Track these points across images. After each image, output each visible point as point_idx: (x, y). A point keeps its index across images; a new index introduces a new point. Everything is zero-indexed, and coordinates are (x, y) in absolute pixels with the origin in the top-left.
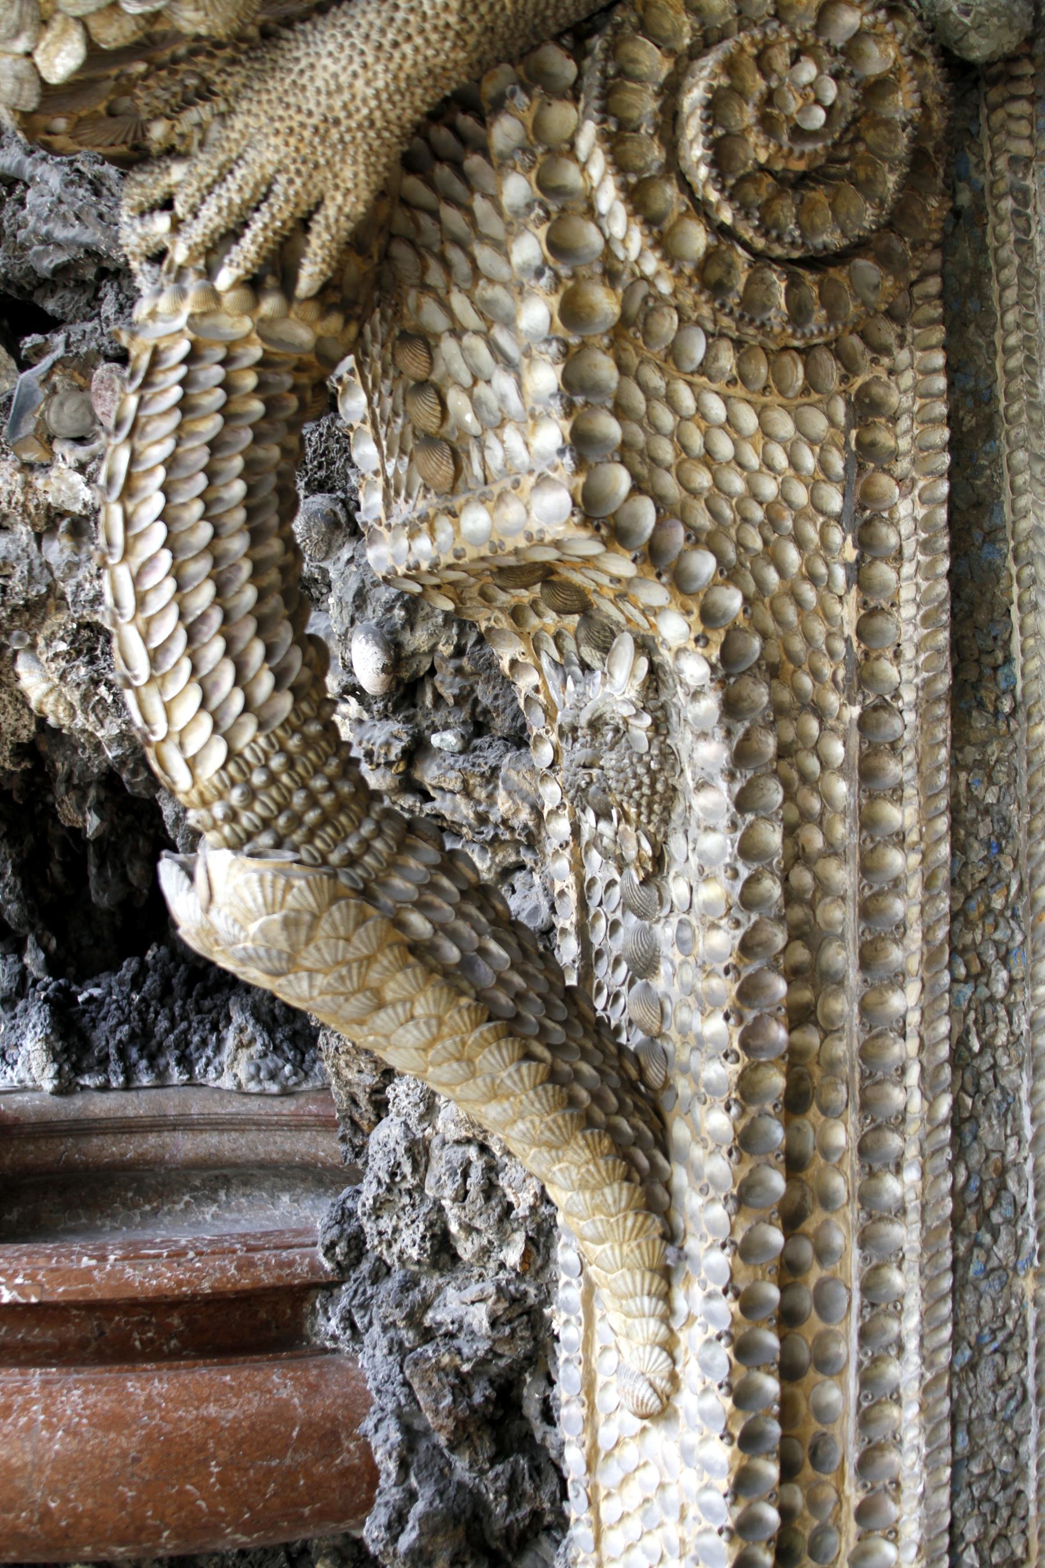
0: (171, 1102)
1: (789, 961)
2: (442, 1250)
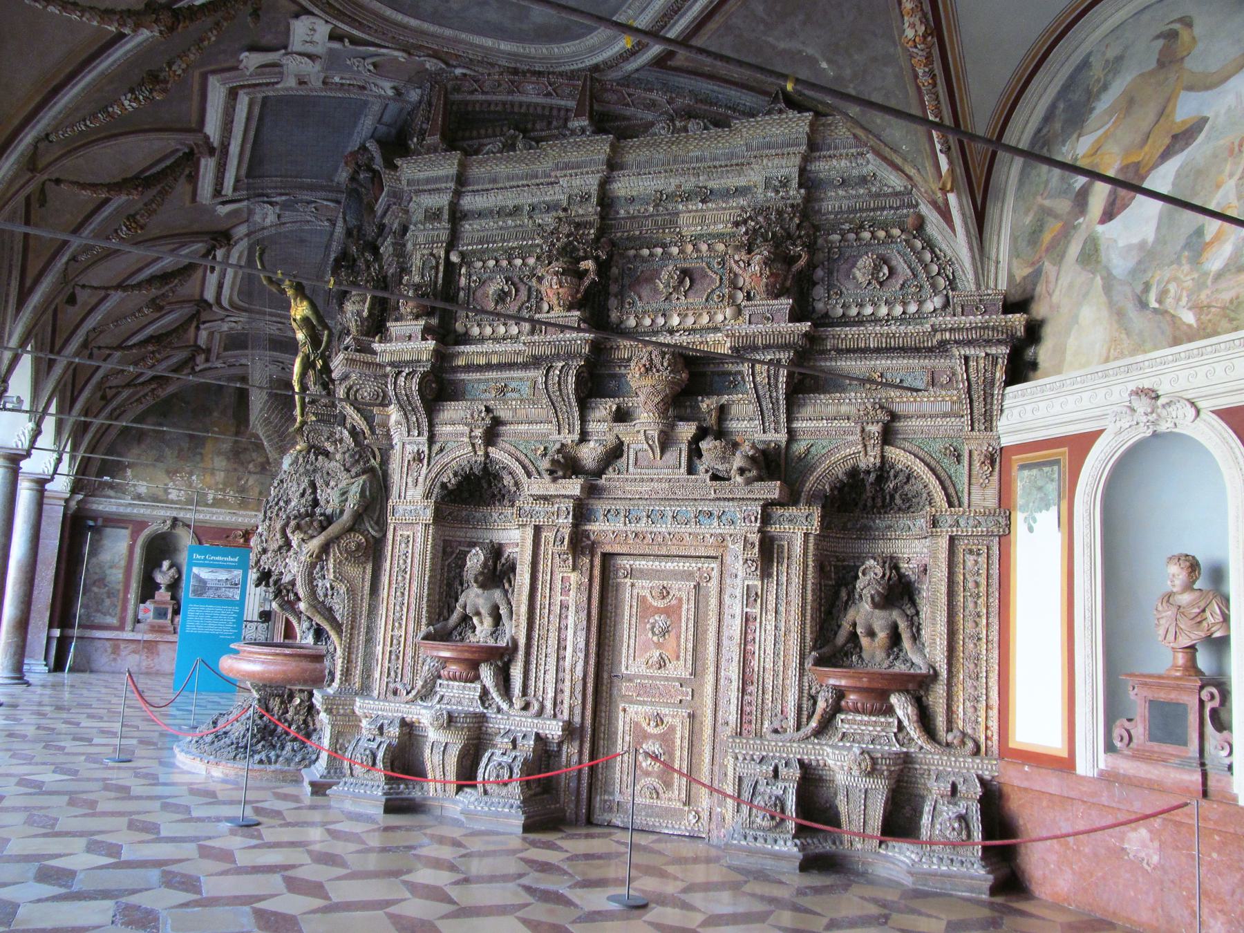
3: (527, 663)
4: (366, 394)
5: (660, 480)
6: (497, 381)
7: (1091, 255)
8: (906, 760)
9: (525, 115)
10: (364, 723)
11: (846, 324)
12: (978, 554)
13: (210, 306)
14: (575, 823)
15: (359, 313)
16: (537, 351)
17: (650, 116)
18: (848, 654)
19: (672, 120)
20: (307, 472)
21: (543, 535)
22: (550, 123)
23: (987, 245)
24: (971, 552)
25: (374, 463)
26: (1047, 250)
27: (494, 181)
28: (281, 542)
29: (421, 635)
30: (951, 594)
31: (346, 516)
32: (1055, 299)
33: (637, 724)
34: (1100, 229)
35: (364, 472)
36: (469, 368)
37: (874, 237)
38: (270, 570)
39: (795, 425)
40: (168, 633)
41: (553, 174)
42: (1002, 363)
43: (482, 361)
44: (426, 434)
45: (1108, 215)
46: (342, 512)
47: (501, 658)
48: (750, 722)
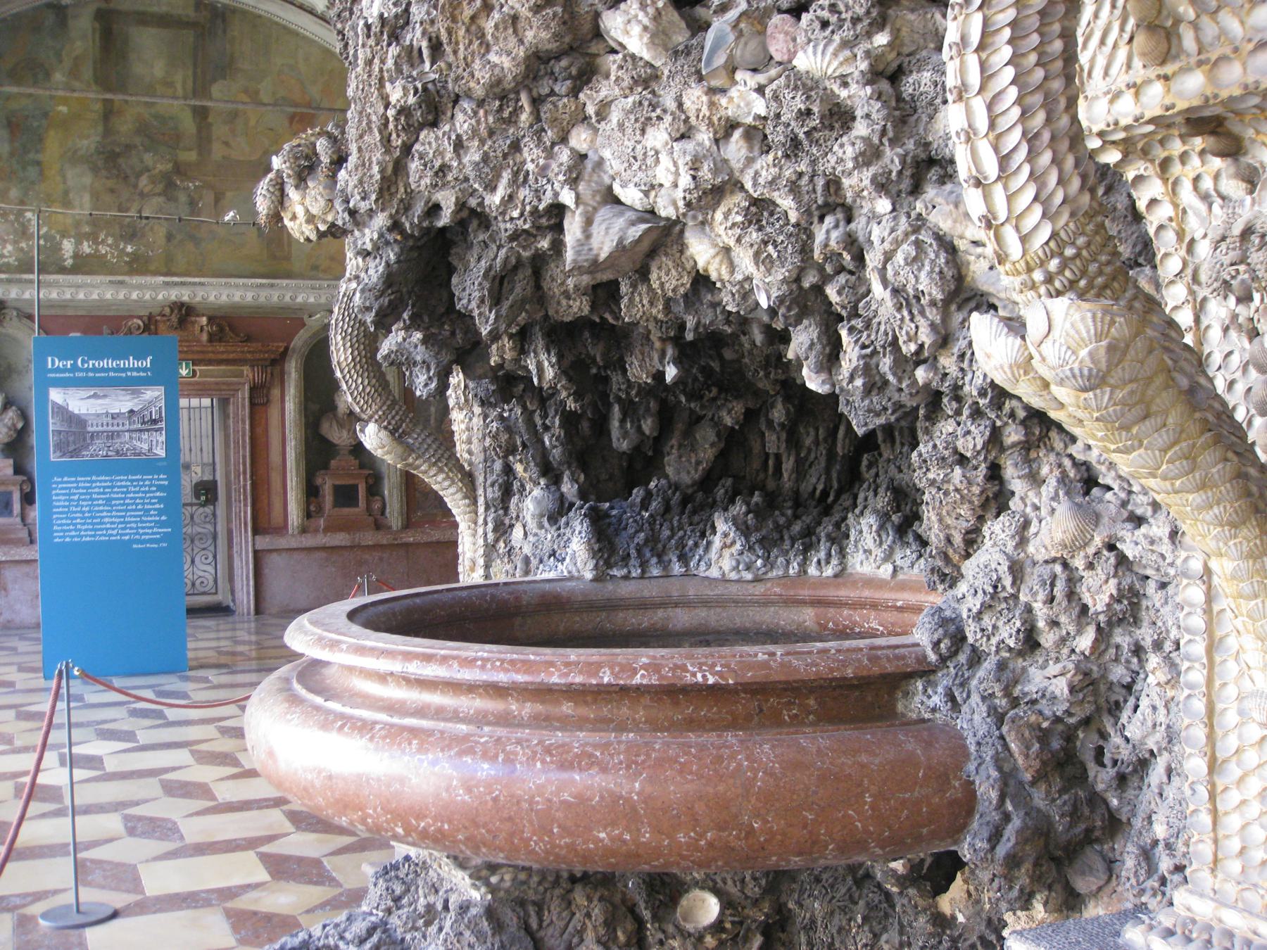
0: (674, 589)
2: (1030, 642)
38: (473, 218)
40: (17, 542)
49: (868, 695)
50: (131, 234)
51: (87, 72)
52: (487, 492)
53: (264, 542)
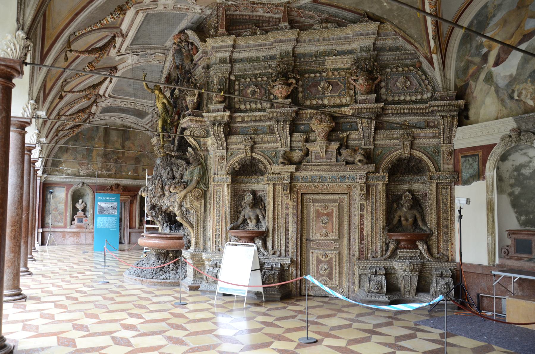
1: (198, 221)
3: (273, 236)
4: (197, 133)
5: (325, 165)
6: (253, 127)
7: (489, 78)
8: (423, 264)
9: (258, 20)
10: (207, 262)
11: (394, 104)
12: (447, 189)
13: (101, 96)
14: (295, 296)
15: (193, 101)
16: (273, 115)
17: (311, 21)
18: (398, 228)
19: (321, 23)
20: (168, 165)
21: (277, 187)
22: (269, 24)
23: (446, 73)
24: (444, 188)
25: (202, 161)
26: (471, 76)
27: (248, 47)
28: (161, 193)
29: (228, 228)
30: (438, 204)
31: (194, 183)
32: (475, 94)
33: (317, 257)
34: (493, 69)
35: (199, 164)
36: (242, 121)
37: (403, 70)
38: (156, 204)
39: (376, 142)
40: (84, 228)
41: (274, 44)
42: (456, 119)
43: (249, 119)
44: (225, 148)
45: (496, 64)
46: (191, 181)
47: (263, 236)
48: (363, 255)
49: (180, 238)
50: (109, 170)
51: (102, 139)
52: (162, 224)
53: (131, 230)
